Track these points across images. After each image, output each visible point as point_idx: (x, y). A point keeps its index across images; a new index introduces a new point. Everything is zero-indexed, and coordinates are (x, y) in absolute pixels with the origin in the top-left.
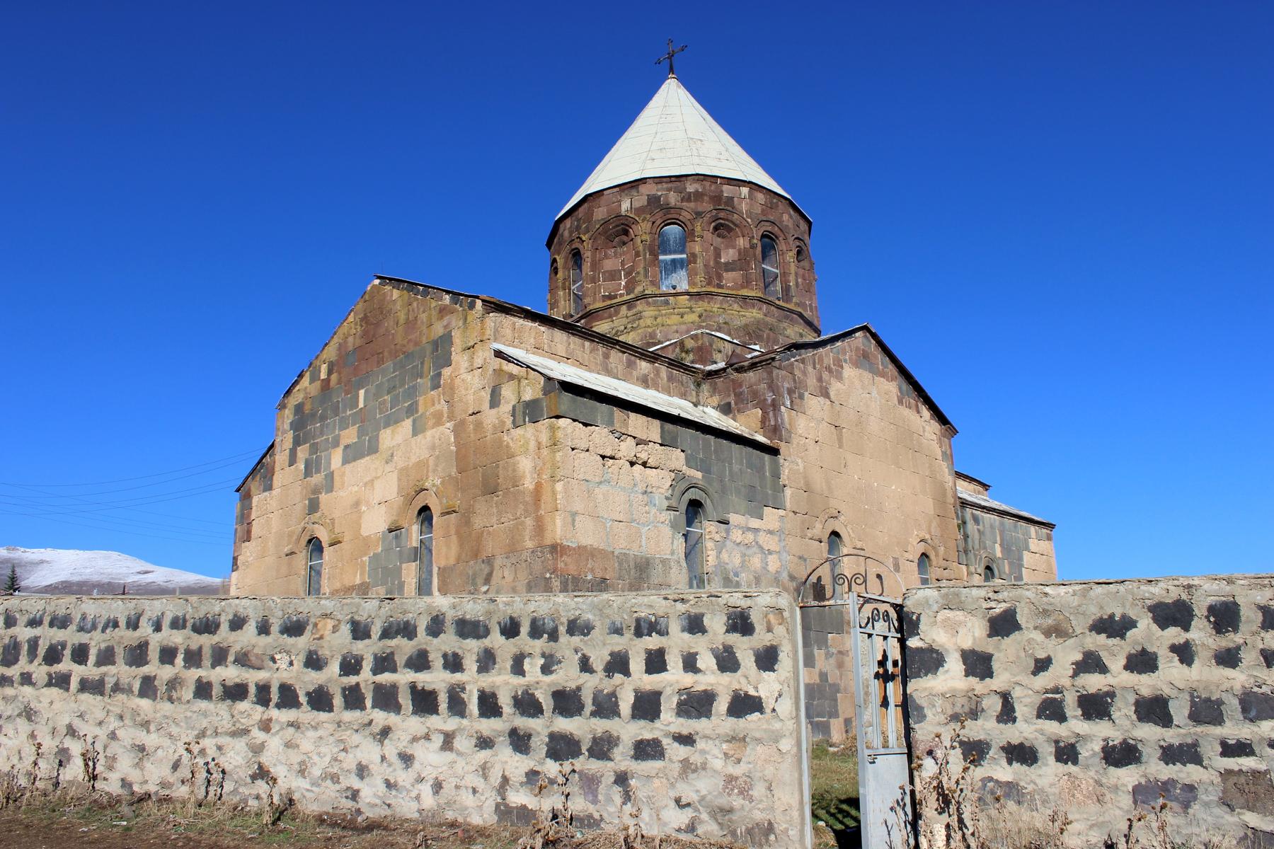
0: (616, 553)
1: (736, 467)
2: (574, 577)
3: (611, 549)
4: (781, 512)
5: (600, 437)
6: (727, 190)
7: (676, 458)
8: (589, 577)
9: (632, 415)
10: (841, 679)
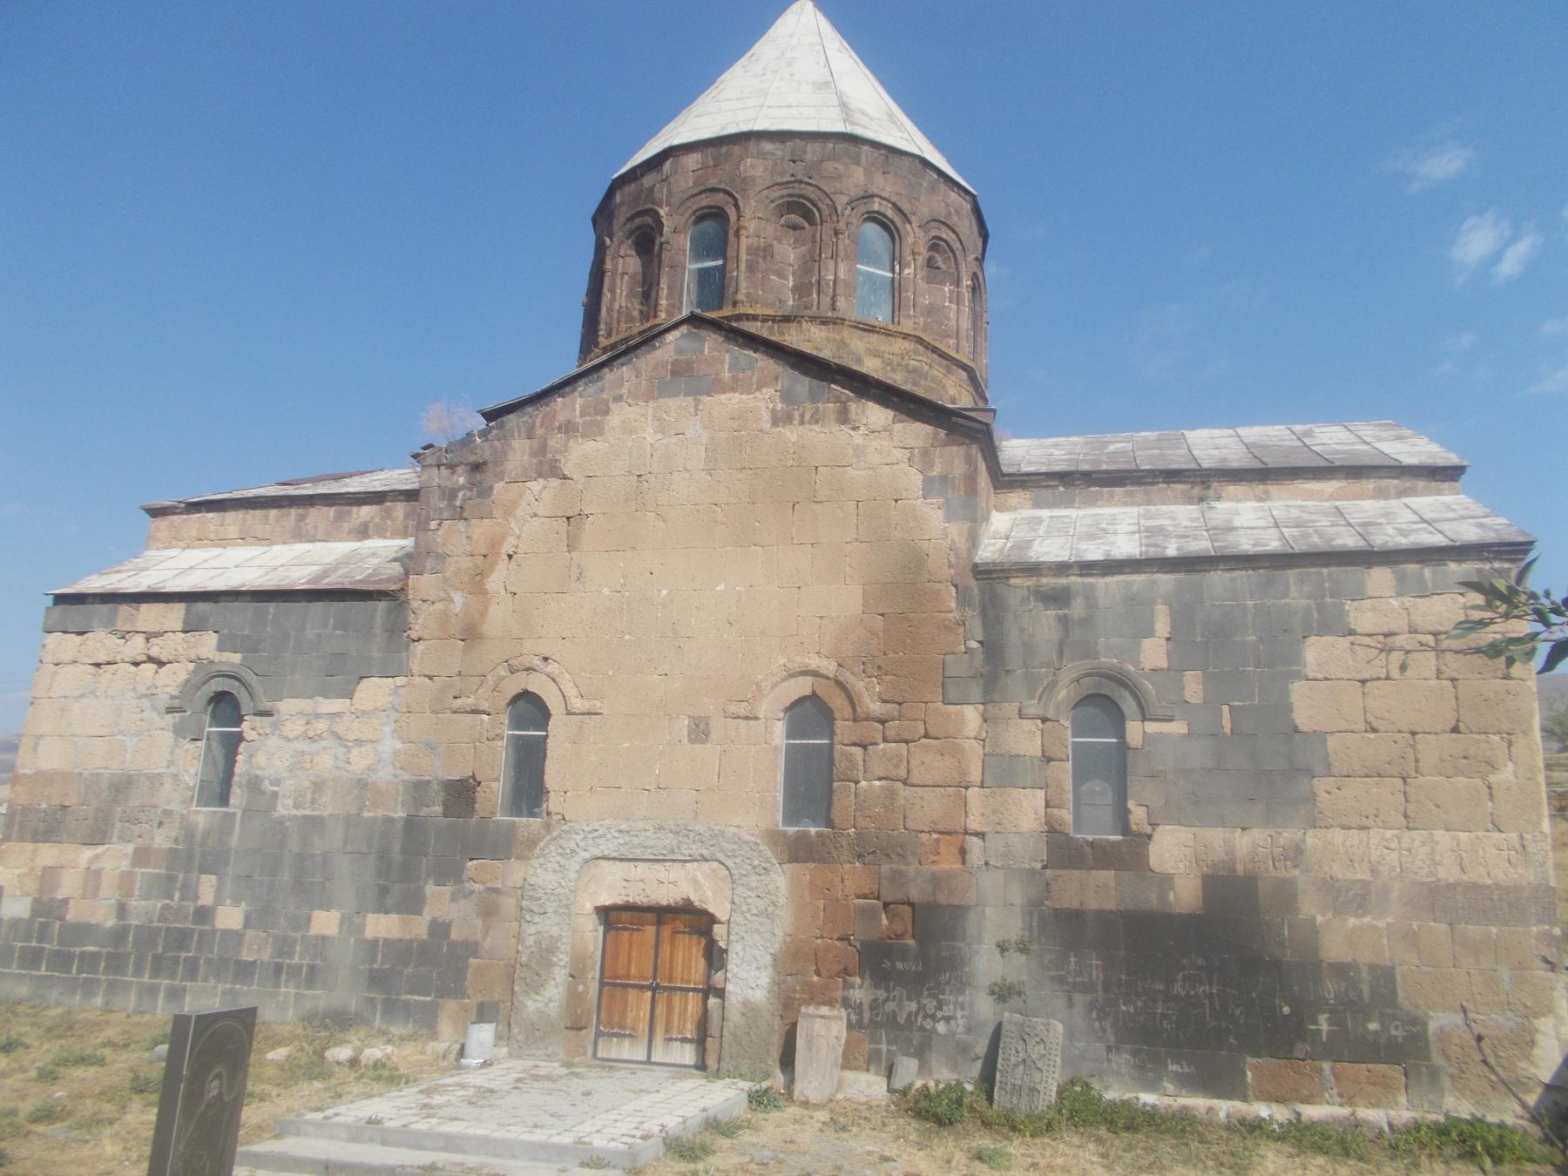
0: (86, 774)
1: (310, 633)
3: (80, 770)
4: (400, 681)
5: (101, 643)
7: (207, 644)
8: (44, 806)
9: (144, 607)
10: (486, 933)
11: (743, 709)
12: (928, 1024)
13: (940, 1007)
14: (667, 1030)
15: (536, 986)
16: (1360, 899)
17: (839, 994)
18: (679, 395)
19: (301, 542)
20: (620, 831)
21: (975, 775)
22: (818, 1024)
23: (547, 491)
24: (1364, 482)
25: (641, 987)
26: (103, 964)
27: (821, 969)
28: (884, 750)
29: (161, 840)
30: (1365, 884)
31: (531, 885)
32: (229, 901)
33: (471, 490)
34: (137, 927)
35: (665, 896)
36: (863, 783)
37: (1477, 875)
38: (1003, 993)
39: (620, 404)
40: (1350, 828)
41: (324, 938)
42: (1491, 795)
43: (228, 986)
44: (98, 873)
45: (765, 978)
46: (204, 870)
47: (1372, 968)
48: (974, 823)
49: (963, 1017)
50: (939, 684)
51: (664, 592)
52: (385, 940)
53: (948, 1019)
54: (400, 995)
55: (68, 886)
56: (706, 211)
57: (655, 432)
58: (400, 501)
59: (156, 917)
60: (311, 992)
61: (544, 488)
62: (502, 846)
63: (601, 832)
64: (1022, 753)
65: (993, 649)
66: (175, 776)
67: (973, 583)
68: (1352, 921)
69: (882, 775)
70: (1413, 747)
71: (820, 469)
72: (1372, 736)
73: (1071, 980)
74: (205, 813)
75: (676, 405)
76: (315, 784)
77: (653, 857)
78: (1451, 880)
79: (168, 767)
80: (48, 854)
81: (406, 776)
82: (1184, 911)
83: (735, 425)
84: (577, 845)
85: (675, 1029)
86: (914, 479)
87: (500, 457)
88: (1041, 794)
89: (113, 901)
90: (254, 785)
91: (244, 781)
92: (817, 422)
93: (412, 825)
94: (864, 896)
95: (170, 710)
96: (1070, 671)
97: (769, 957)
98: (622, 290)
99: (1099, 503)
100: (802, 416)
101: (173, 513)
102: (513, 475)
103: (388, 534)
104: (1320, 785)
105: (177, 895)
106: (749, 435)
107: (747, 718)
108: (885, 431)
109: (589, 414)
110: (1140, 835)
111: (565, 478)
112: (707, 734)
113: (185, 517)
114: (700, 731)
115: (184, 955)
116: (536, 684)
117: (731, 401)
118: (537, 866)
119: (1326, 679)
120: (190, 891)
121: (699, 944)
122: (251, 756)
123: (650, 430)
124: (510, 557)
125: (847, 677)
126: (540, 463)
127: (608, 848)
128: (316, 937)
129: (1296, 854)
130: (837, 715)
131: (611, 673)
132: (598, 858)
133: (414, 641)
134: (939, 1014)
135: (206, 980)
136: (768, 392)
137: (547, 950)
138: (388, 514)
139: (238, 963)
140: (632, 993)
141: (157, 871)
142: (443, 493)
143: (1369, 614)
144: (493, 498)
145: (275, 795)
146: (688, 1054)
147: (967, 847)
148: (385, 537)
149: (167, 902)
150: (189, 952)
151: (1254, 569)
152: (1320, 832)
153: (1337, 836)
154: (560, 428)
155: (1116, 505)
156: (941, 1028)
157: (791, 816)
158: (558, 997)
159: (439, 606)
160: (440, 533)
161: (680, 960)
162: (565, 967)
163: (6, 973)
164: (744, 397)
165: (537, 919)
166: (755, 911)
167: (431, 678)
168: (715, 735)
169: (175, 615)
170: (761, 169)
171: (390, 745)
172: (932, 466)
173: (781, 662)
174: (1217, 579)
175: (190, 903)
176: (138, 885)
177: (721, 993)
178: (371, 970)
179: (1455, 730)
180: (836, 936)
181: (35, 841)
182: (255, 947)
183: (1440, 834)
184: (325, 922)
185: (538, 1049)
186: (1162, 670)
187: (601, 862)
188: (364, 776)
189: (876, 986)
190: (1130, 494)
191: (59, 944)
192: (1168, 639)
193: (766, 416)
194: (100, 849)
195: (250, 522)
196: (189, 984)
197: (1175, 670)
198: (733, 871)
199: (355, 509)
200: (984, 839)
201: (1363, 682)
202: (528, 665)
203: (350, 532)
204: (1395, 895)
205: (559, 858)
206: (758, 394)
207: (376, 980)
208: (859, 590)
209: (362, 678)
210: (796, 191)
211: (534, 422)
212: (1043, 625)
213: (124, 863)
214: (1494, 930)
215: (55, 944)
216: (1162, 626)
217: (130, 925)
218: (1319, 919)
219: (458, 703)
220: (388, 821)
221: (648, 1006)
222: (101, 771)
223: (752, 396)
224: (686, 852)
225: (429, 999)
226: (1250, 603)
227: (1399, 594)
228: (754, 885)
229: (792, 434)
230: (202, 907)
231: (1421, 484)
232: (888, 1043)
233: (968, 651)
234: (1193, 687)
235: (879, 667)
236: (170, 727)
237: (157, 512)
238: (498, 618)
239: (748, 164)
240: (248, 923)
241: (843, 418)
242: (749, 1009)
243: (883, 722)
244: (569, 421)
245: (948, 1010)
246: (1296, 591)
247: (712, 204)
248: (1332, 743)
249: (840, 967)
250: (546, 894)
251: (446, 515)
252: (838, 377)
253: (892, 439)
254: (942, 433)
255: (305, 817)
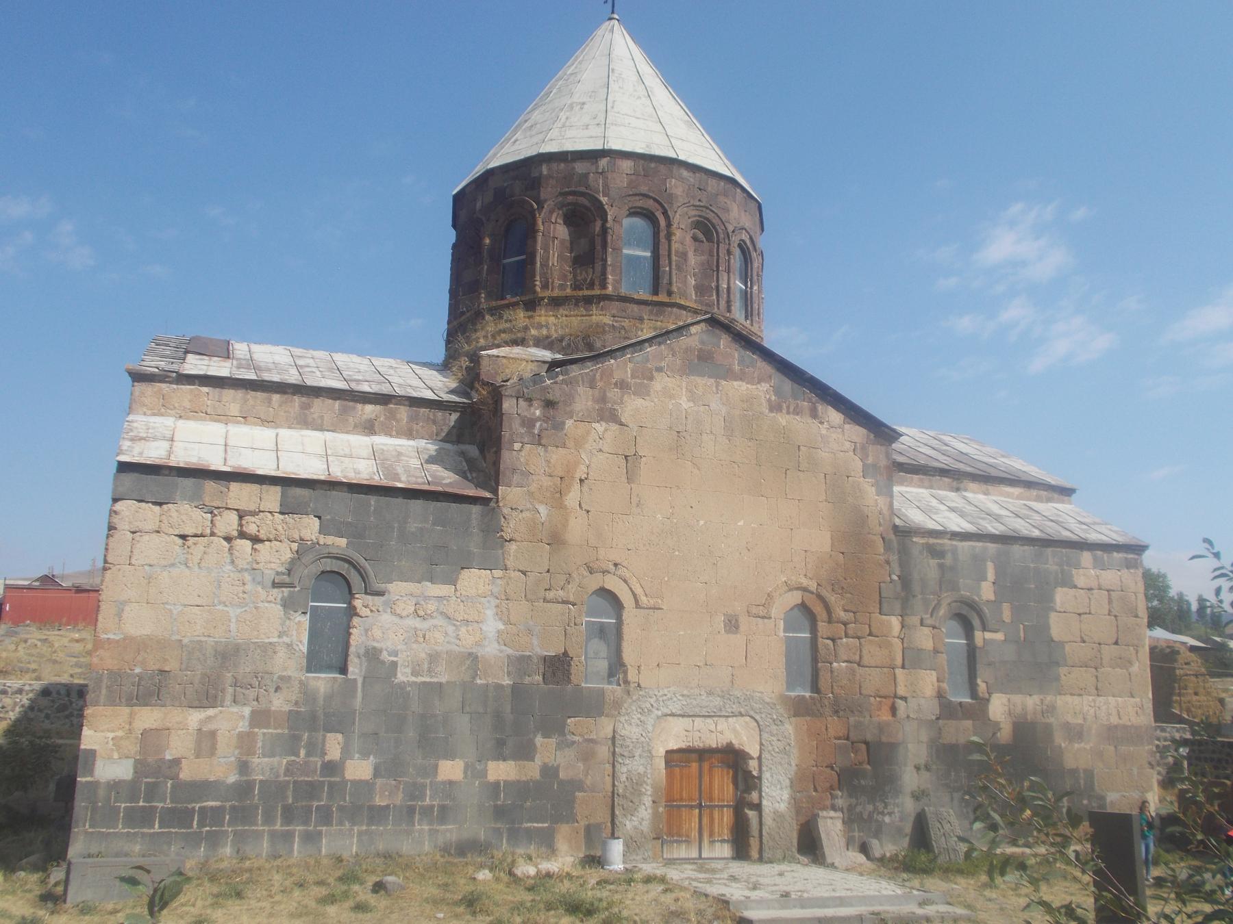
1: (413, 526)
2: (111, 672)
3: (178, 637)
4: (498, 573)
6: (580, 167)
7: (309, 527)
8: (138, 670)
9: (235, 486)
10: (587, 774)
11: (762, 612)
12: (880, 818)
13: (886, 807)
14: (711, 834)
15: (632, 812)
16: (1076, 733)
17: (828, 803)
18: (705, 376)
19: (307, 429)
20: (683, 696)
21: (899, 661)
22: (829, 821)
23: (609, 432)
24: (1032, 491)
25: (692, 807)
26: (227, 817)
27: (817, 787)
28: (847, 643)
29: (279, 703)
30: (1081, 726)
31: (621, 736)
32: (357, 756)
33: (546, 422)
34: (261, 781)
35: (713, 741)
36: (835, 664)
37: (1125, 721)
38: (917, 796)
39: (661, 374)
40: (1074, 695)
41: (451, 783)
42: (1130, 678)
43: (364, 828)
44: (213, 734)
45: (786, 795)
46: (329, 729)
47: (1085, 771)
48: (901, 691)
49: (899, 811)
50: (878, 602)
51: (702, 522)
52: (505, 781)
53: (890, 814)
54: (522, 823)
55: (178, 746)
56: (639, 210)
57: (689, 401)
58: (404, 405)
59: (282, 771)
60: (444, 827)
61: (606, 430)
62: (594, 706)
63: (669, 696)
64: (924, 648)
65: (905, 581)
66: (289, 646)
67: (892, 537)
68: (1076, 745)
69: (846, 659)
70: (1099, 651)
71: (801, 447)
72: (1083, 644)
73: (952, 785)
74: (325, 678)
75: (703, 383)
76: (430, 655)
77: (707, 714)
78: (1115, 723)
79: (279, 637)
80: (148, 718)
81: (510, 651)
82: (1004, 743)
83: (745, 406)
84: (652, 705)
85: (716, 834)
86: (858, 464)
87: (570, 399)
88: (934, 673)
89: (233, 759)
90: (372, 655)
91: (362, 651)
92: (798, 414)
93: (517, 691)
94: (839, 738)
95: (275, 585)
96: (947, 598)
97: (788, 781)
98: (553, 251)
99: (905, 484)
100: (788, 407)
101: (160, 381)
102: (581, 414)
103: (394, 433)
104: (1063, 670)
105: (303, 752)
106: (754, 415)
107: (763, 617)
108: (840, 428)
109: (638, 377)
110: (983, 699)
111: (622, 424)
112: (737, 627)
113: (175, 386)
114: (732, 625)
115: (315, 804)
116: (612, 584)
117: (738, 388)
118: (624, 721)
119: (1065, 612)
120: (315, 748)
121: (728, 773)
122: (366, 631)
123: (684, 398)
124: (581, 480)
125: (824, 593)
126: (601, 410)
127: (675, 707)
128: (444, 783)
129: (1052, 709)
130: (819, 618)
131: (666, 579)
132: (666, 715)
133: (506, 541)
134: (886, 811)
135: (341, 823)
136: (765, 386)
137: (637, 783)
138: (392, 416)
139: (371, 808)
140: (684, 811)
141: (279, 731)
142: (523, 422)
143: (1082, 577)
144: (565, 431)
145: (394, 664)
146: (725, 850)
147: (897, 705)
148: (391, 436)
149: (293, 758)
150: (320, 801)
151: (1034, 546)
152: (1063, 697)
153: (1069, 698)
154: (616, 384)
155: (914, 487)
156: (887, 819)
157: (790, 685)
158: (648, 817)
159: (526, 514)
160: (523, 454)
161: (716, 786)
162: (651, 795)
163: (109, 833)
164: (749, 386)
165: (627, 761)
166: (777, 750)
167: (524, 573)
168: (742, 628)
169: (272, 497)
170: (681, 189)
171: (492, 626)
172: (868, 456)
173: (783, 580)
174: (1017, 550)
175: (316, 759)
176: (260, 744)
177: (758, 807)
178: (496, 806)
179: (1116, 643)
180: (825, 765)
181: (129, 704)
182: (387, 793)
183: (1110, 699)
184: (451, 770)
185: (637, 855)
186: (992, 601)
187: (670, 718)
188: (474, 651)
189: (850, 796)
190: (921, 480)
191: (172, 802)
192: (994, 583)
193: (765, 404)
194: (211, 712)
195: (251, 402)
196: (324, 828)
197: (997, 603)
198: (761, 723)
199: (359, 406)
200: (906, 702)
201: (1079, 614)
202: (605, 568)
203: (356, 426)
204: (1094, 731)
205: (639, 716)
206: (759, 386)
207: (500, 813)
208: (828, 535)
209: (463, 568)
210: (703, 214)
211: (595, 375)
212: (928, 568)
213: (241, 724)
214: (1132, 748)
215: (168, 801)
216: (991, 575)
217: (256, 780)
218: (1063, 745)
219: (550, 595)
220: (499, 687)
221: (697, 820)
222: (203, 639)
223: (754, 387)
224: (729, 710)
225: (546, 825)
226: (1032, 565)
227: (1094, 568)
228: (775, 732)
229: (783, 419)
230: (330, 762)
231: (1056, 496)
232: (859, 831)
233: (892, 581)
234: (1007, 614)
235: (843, 588)
236: (278, 600)
237: (139, 377)
238: (576, 528)
239: (673, 184)
240: (377, 773)
241: (814, 414)
242: (778, 815)
243: (845, 624)
244: (623, 380)
245: (890, 809)
246: (1051, 561)
247: (645, 207)
248: (1067, 648)
249: (828, 785)
250: (633, 742)
251: (526, 440)
252: (807, 384)
253: (844, 435)
254: (872, 436)
255: (424, 683)
